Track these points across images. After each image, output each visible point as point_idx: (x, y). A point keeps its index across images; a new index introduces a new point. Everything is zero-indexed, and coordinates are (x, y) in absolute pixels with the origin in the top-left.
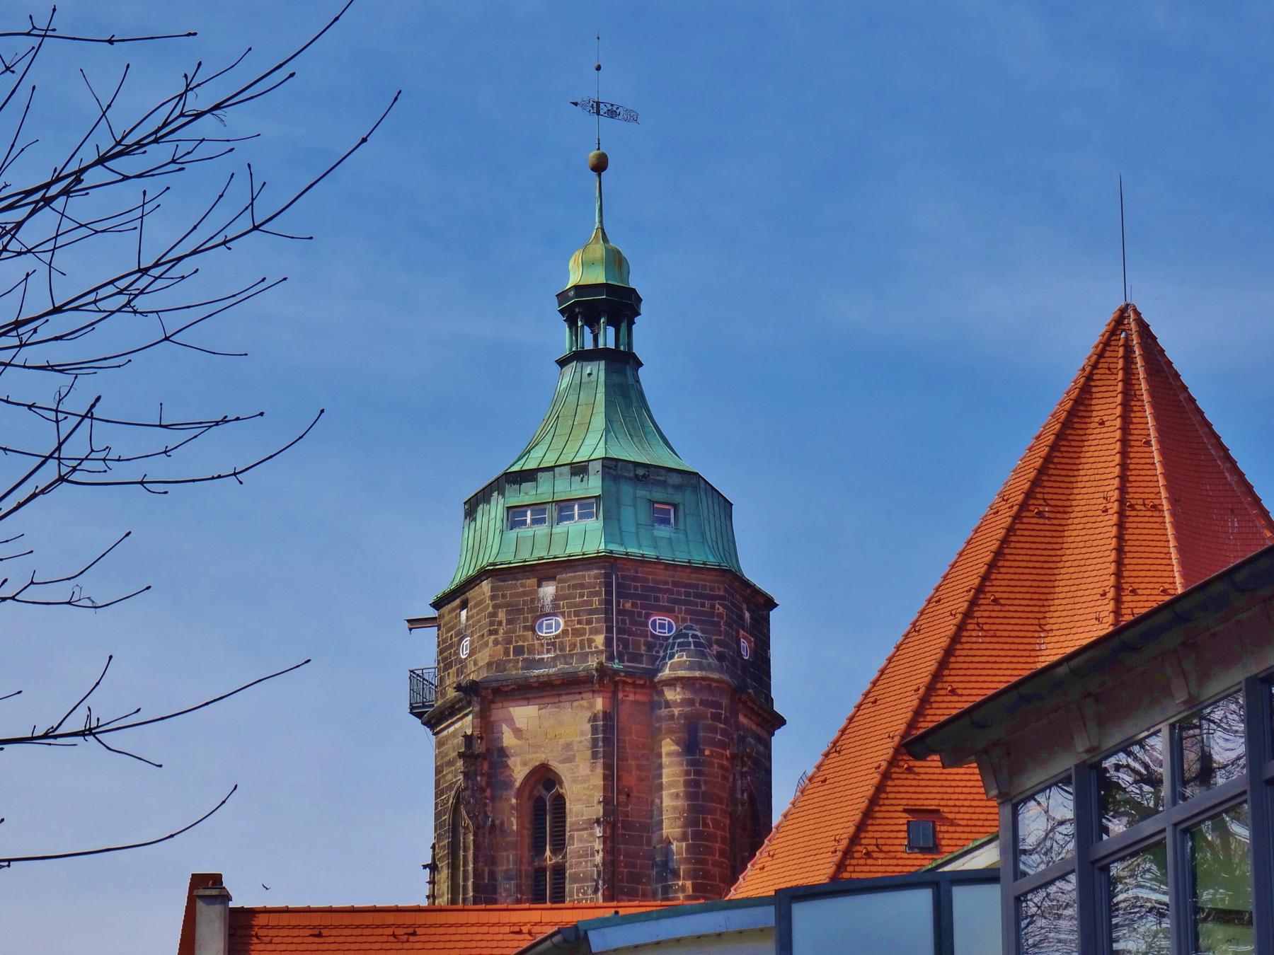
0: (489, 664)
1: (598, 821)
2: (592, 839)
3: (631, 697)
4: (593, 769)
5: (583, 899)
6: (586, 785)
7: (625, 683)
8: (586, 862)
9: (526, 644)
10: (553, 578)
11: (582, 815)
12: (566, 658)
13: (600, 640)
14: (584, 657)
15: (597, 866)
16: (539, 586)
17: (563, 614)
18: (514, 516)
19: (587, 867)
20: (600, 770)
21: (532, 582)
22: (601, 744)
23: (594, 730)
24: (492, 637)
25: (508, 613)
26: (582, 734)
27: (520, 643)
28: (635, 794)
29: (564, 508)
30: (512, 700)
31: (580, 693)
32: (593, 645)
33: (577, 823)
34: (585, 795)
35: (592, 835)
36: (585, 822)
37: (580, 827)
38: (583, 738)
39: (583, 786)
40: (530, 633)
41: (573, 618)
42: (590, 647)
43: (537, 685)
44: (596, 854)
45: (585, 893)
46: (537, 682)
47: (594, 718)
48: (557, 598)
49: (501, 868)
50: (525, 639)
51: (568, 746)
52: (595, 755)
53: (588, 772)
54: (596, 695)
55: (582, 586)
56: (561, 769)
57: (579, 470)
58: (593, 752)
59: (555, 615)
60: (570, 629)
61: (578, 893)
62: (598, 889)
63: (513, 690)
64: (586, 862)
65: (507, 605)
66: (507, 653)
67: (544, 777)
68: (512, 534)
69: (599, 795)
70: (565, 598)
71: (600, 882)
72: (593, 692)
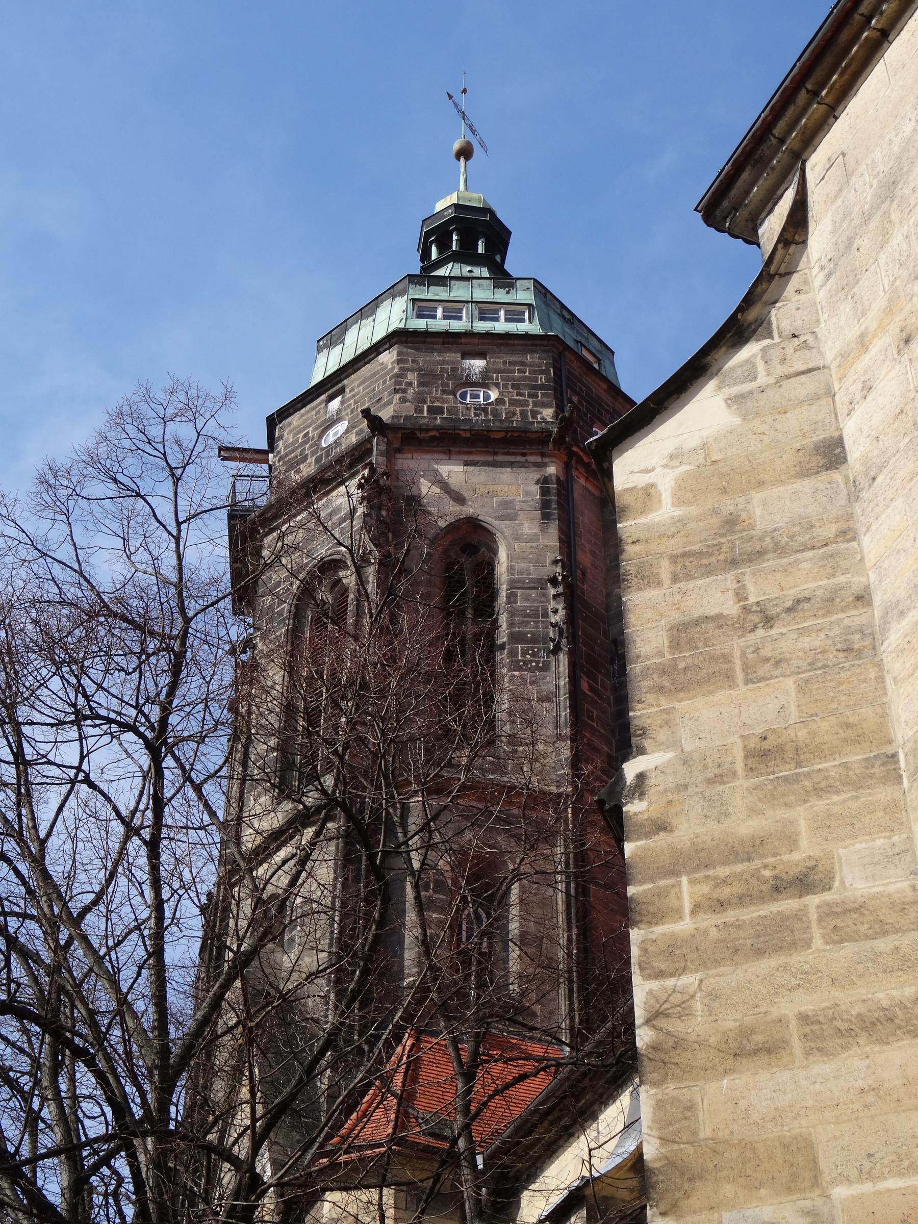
1: (553, 581)
2: (544, 599)
3: (582, 481)
4: (544, 530)
5: (531, 662)
6: (535, 545)
7: (580, 460)
8: (536, 623)
9: (445, 406)
10: (481, 355)
11: (530, 574)
15: (554, 625)
16: (463, 358)
17: (497, 385)
19: (537, 627)
20: (553, 530)
21: (453, 356)
22: (554, 506)
23: (544, 492)
24: (398, 396)
25: (419, 376)
26: (527, 493)
27: (437, 404)
28: (589, 575)
30: (428, 452)
31: (524, 455)
32: (539, 417)
33: (519, 581)
34: (531, 553)
35: (544, 595)
36: (531, 581)
37: (526, 586)
38: (529, 499)
39: (529, 544)
40: (451, 397)
41: (511, 390)
42: (534, 417)
43: (468, 435)
44: (551, 614)
45: (533, 655)
46: (470, 430)
50: (444, 401)
51: (506, 504)
52: (546, 517)
53: (536, 530)
54: (546, 460)
55: (522, 364)
58: (542, 513)
59: (485, 386)
60: (506, 399)
61: (523, 654)
62: (561, 649)
63: (433, 438)
64: (536, 623)
65: (419, 370)
66: (419, 410)
70: (497, 371)
71: (564, 641)
72: (543, 455)
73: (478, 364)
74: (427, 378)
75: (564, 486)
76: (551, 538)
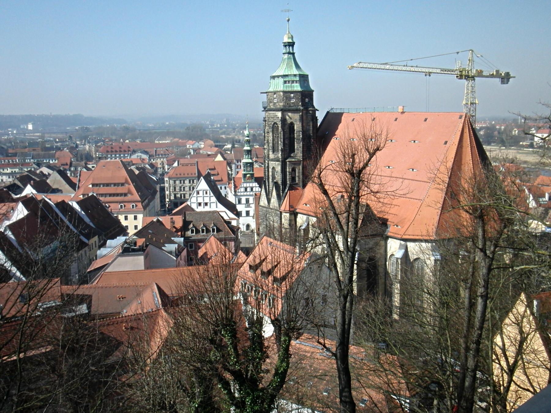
0: (283, 106)
12: (295, 106)
13: (300, 103)
14: (298, 106)
18: (285, 82)
20: (301, 123)
21: (289, 94)
29: (293, 82)
47: (300, 116)
48: (294, 96)
49: (286, 137)
51: (296, 119)
56: (295, 123)
57: (295, 75)
67: (292, 124)
68: (286, 84)
69: (301, 127)
73: (292, 95)
74: (287, 98)
75: (302, 115)
76: (300, 125)
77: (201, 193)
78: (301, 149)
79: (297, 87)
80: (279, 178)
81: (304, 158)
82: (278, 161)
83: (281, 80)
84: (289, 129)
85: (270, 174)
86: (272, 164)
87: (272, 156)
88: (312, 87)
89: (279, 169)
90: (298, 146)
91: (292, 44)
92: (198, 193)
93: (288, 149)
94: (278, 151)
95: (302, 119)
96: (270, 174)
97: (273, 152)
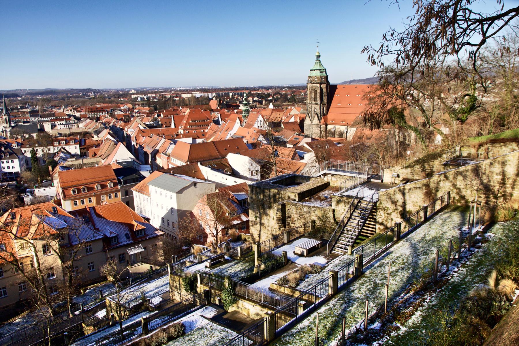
77: (259, 121)
78: (326, 100)
79: (324, 74)
80: (318, 111)
81: (327, 103)
82: (317, 104)
83: (319, 71)
84: (321, 90)
85: (313, 110)
86: (314, 106)
87: (314, 102)
88: (328, 74)
89: (318, 107)
90: (325, 98)
91: (319, 56)
92: (258, 122)
93: (322, 100)
94: (317, 101)
95: (327, 87)
96: (313, 110)
97: (314, 101)
